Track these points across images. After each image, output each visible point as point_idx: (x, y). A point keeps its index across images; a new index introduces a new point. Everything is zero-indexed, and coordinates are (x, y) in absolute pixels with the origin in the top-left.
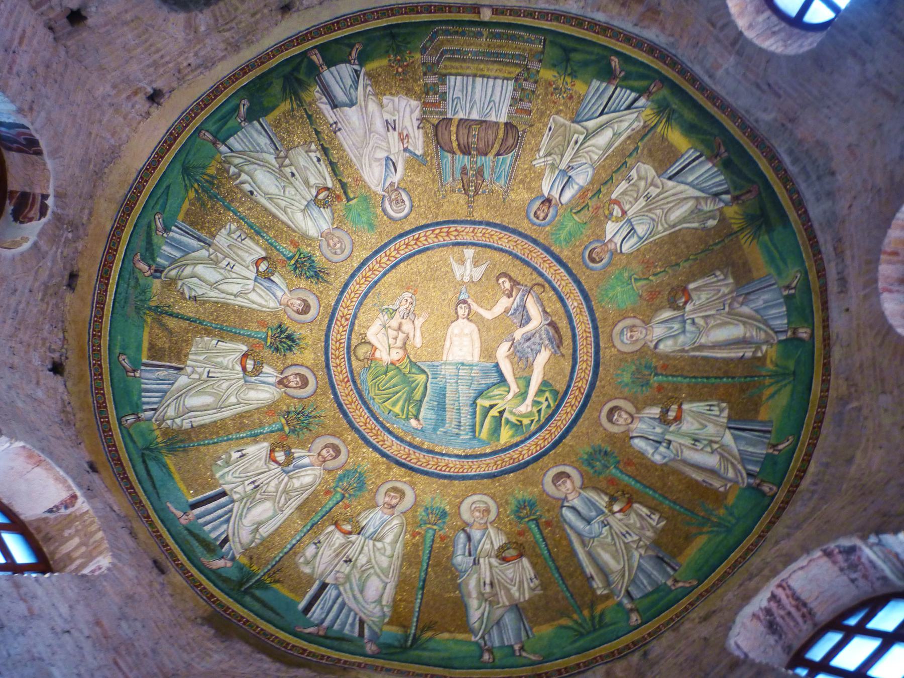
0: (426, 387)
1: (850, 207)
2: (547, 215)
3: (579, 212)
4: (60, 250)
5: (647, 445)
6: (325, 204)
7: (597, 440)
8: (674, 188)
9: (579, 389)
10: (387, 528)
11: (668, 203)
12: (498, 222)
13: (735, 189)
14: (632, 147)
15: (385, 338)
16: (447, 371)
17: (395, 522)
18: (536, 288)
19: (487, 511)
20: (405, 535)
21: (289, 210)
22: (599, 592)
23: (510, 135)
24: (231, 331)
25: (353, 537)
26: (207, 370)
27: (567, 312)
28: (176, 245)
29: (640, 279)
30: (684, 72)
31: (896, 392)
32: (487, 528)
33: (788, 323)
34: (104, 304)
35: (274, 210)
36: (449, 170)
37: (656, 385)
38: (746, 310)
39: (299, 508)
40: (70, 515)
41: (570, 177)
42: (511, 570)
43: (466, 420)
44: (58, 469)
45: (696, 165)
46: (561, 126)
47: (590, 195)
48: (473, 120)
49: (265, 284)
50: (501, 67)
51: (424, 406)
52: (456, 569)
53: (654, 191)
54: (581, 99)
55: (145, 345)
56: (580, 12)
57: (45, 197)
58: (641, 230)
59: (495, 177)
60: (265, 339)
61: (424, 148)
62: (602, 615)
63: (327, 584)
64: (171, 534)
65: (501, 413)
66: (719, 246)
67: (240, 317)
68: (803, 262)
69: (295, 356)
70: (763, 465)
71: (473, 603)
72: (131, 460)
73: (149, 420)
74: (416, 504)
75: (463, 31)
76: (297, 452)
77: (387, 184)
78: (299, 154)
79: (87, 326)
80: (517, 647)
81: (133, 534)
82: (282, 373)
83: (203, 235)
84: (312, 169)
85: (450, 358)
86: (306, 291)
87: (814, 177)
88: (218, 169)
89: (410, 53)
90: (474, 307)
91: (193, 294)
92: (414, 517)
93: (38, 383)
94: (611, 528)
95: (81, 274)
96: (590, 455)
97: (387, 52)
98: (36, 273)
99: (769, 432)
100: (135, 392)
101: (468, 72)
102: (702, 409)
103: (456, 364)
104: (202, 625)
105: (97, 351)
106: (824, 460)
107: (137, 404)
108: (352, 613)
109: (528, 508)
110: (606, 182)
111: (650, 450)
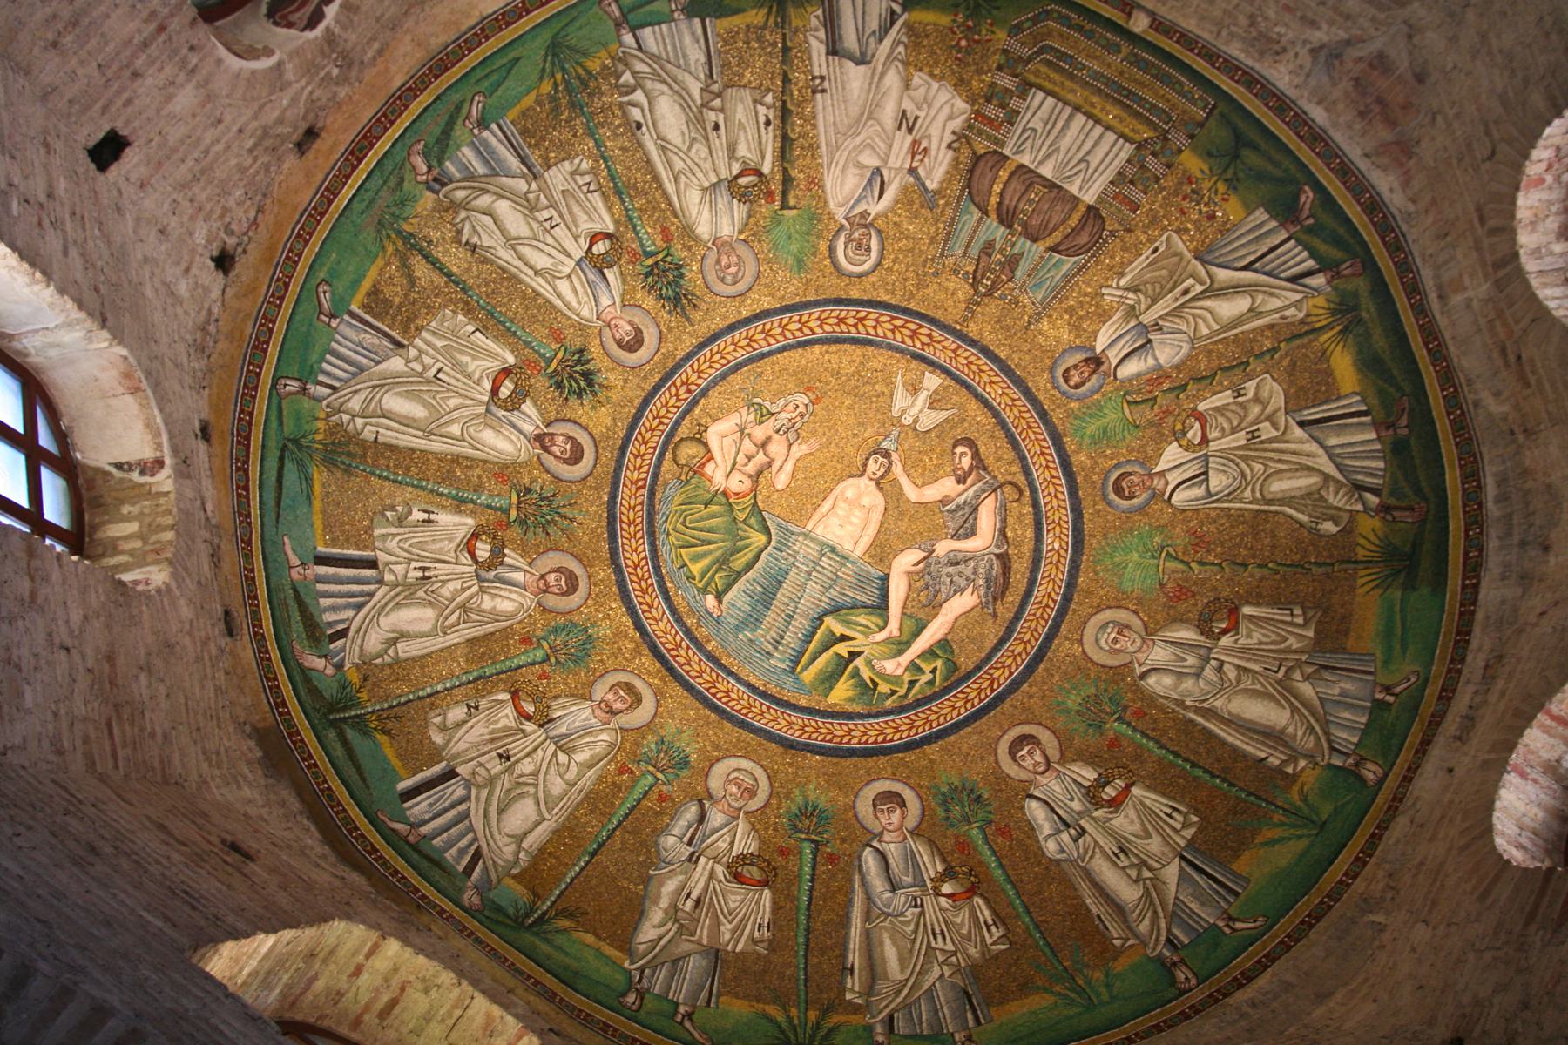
0: (758, 556)
1: (1543, 614)
2: (1083, 383)
4: (309, 88)
5: (1047, 819)
6: (742, 195)
7: (976, 773)
8: (1301, 442)
9: (993, 680)
10: (588, 739)
11: (1279, 461)
12: (1002, 355)
13: (1392, 494)
14: (1268, 344)
15: (734, 450)
16: (804, 549)
17: (604, 737)
18: (1008, 489)
19: (752, 792)
20: (609, 763)
21: (683, 179)
22: (848, 996)
23: (1088, 229)
24: (503, 324)
25: (530, 727)
26: (439, 365)
27: (1037, 551)
29: (1176, 559)
30: (1405, 267)
32: (738, 818)
34: (335, 196)
35: (660, 167)
36: (964, 235)
37: (1111, 734)
38: (1306, 689)
39: (472, 642)
40: (142, 485)
41: (1150, 341)
42: (739, 898)
43: (792, 639)
44: (156, 412)
45: (1352, 425)
46: (1176, 254)
49: (590, 276)
50: (1124, 115)
51: (741, 584)
53: (1267, 432)
54: (1224, 230)
55: (366, 285)
56: (1291, 93)
58: (1217, 482)
59: (1031, 282)
60: (549, 361)
61: (941, 183)
62: (831, 1031)
63: (458, 775)
65: (854, 655)
67: (527, 308)
69: (580, 409)
70: (1197, 938)
71: (656, 915)
72: (263, 446)
73: (319, 400)
74: (648, 726)
75: (1091, 31)
76: (511, 557)
77: (856, 211)
78: (742, 100)
79: (297, 217)
80: (682, 1009)
81: (215, 558)
82: (548, 426)
83: (534, 157)
84: (751, 132)
85: (819, 530)
86: (649, 317)
87: (1516, 539)
88: (604, 67)
89: (991, 25)
90: (898, 470)
91: (475, 240)
92: (637, 744)
93: (187, 270)
94: (922, 913)
95: (324, 135)
97: (957, 6)
98: (261, 108)
99: (1237, 894)
101: (1070, 97)
102: (1157, 808)
103: (823, 544)
104: (250, 737)
105: (292, 261)
106: (1289, 977)
107: (312, 366)
108: (470, 836)
110: (1204, 378)
111: (1047, 829)
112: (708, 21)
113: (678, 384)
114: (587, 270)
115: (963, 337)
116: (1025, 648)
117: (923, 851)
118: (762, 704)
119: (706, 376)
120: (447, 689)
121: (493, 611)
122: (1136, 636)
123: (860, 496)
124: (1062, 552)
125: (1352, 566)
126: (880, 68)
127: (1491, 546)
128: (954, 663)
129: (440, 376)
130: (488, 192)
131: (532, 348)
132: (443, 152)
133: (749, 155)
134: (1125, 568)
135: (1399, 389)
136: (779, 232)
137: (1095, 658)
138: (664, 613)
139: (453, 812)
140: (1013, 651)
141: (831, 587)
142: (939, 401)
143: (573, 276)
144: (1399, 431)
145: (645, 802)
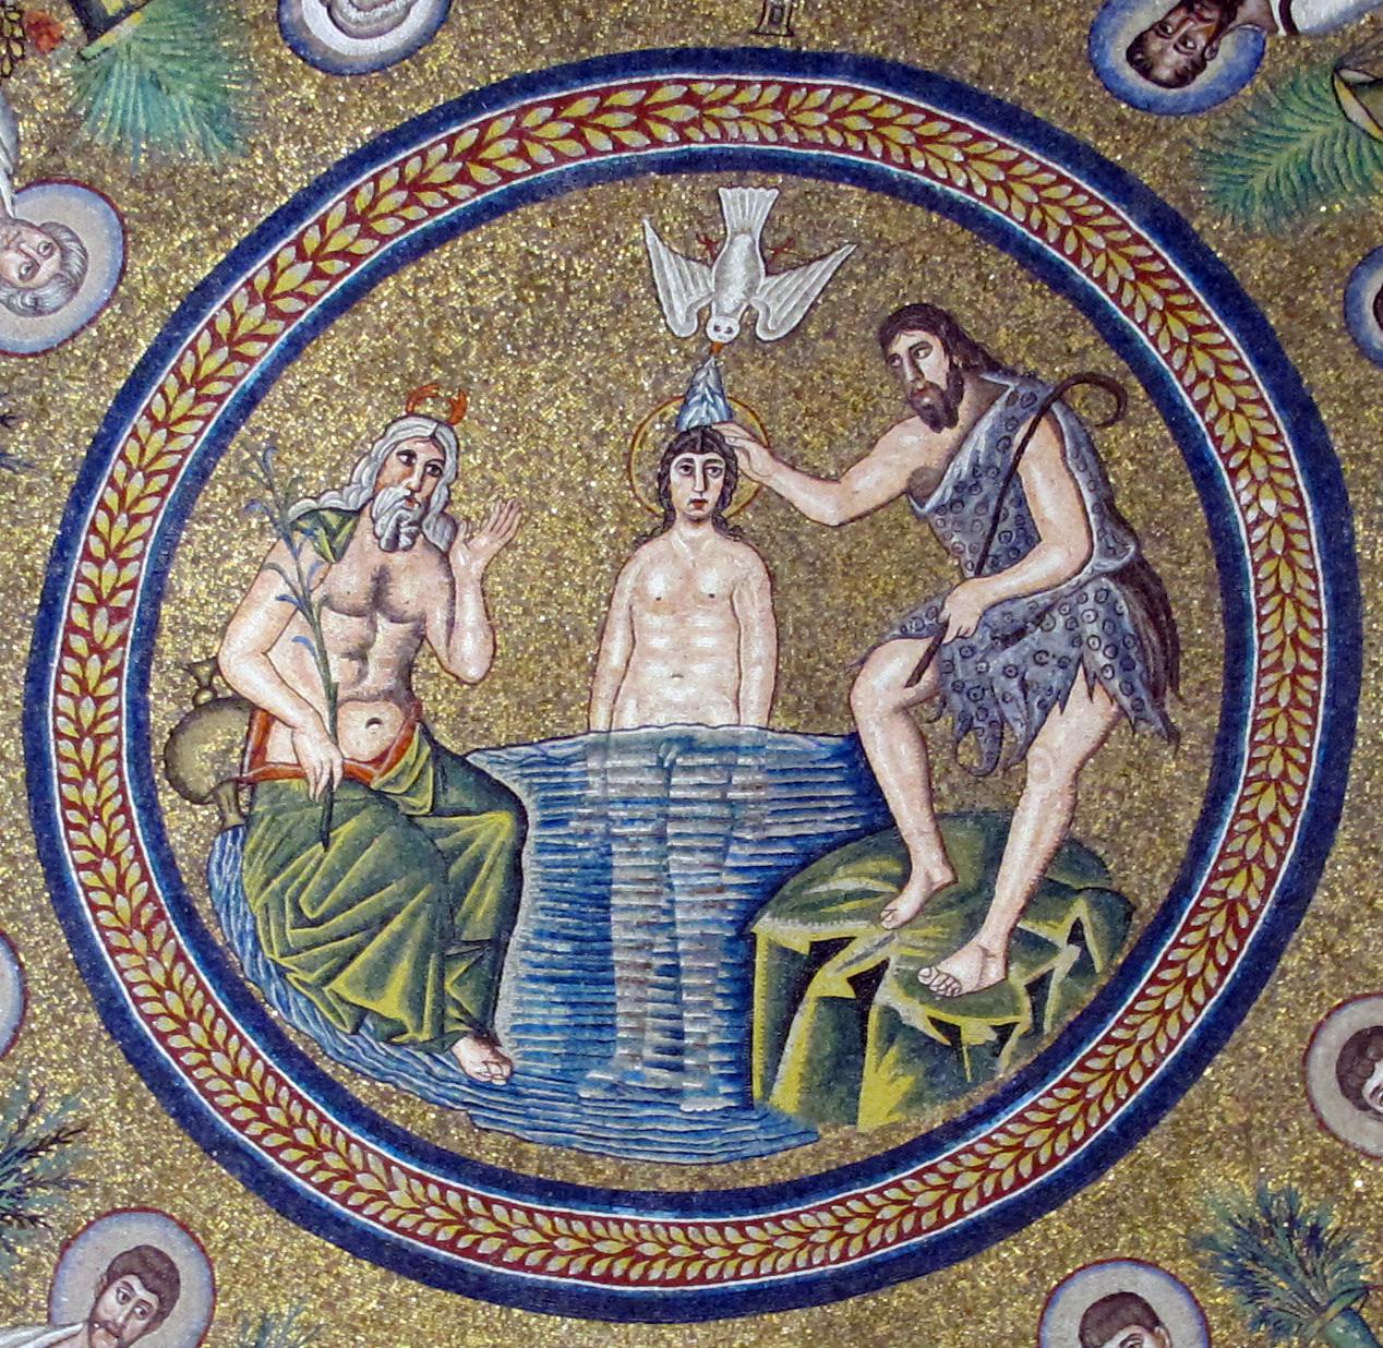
0: (516, 872)
9: (1233, 903)
15: (311, 662)
43: (704, 1027)
51: (515, 964)
65: (867, 983)
85: (629, 718)
90: (756, 462)
103: (653, 745)
113: (80, 618)
116: (1282, 799)
118: (720, 1228)
119: (135, 549)
123: (689, 577)
128: (1118, 894)
136: (120, 95)
138: (388, 1164)
140: (1254, 815)
141: (728, 840)
142: (791, 242)
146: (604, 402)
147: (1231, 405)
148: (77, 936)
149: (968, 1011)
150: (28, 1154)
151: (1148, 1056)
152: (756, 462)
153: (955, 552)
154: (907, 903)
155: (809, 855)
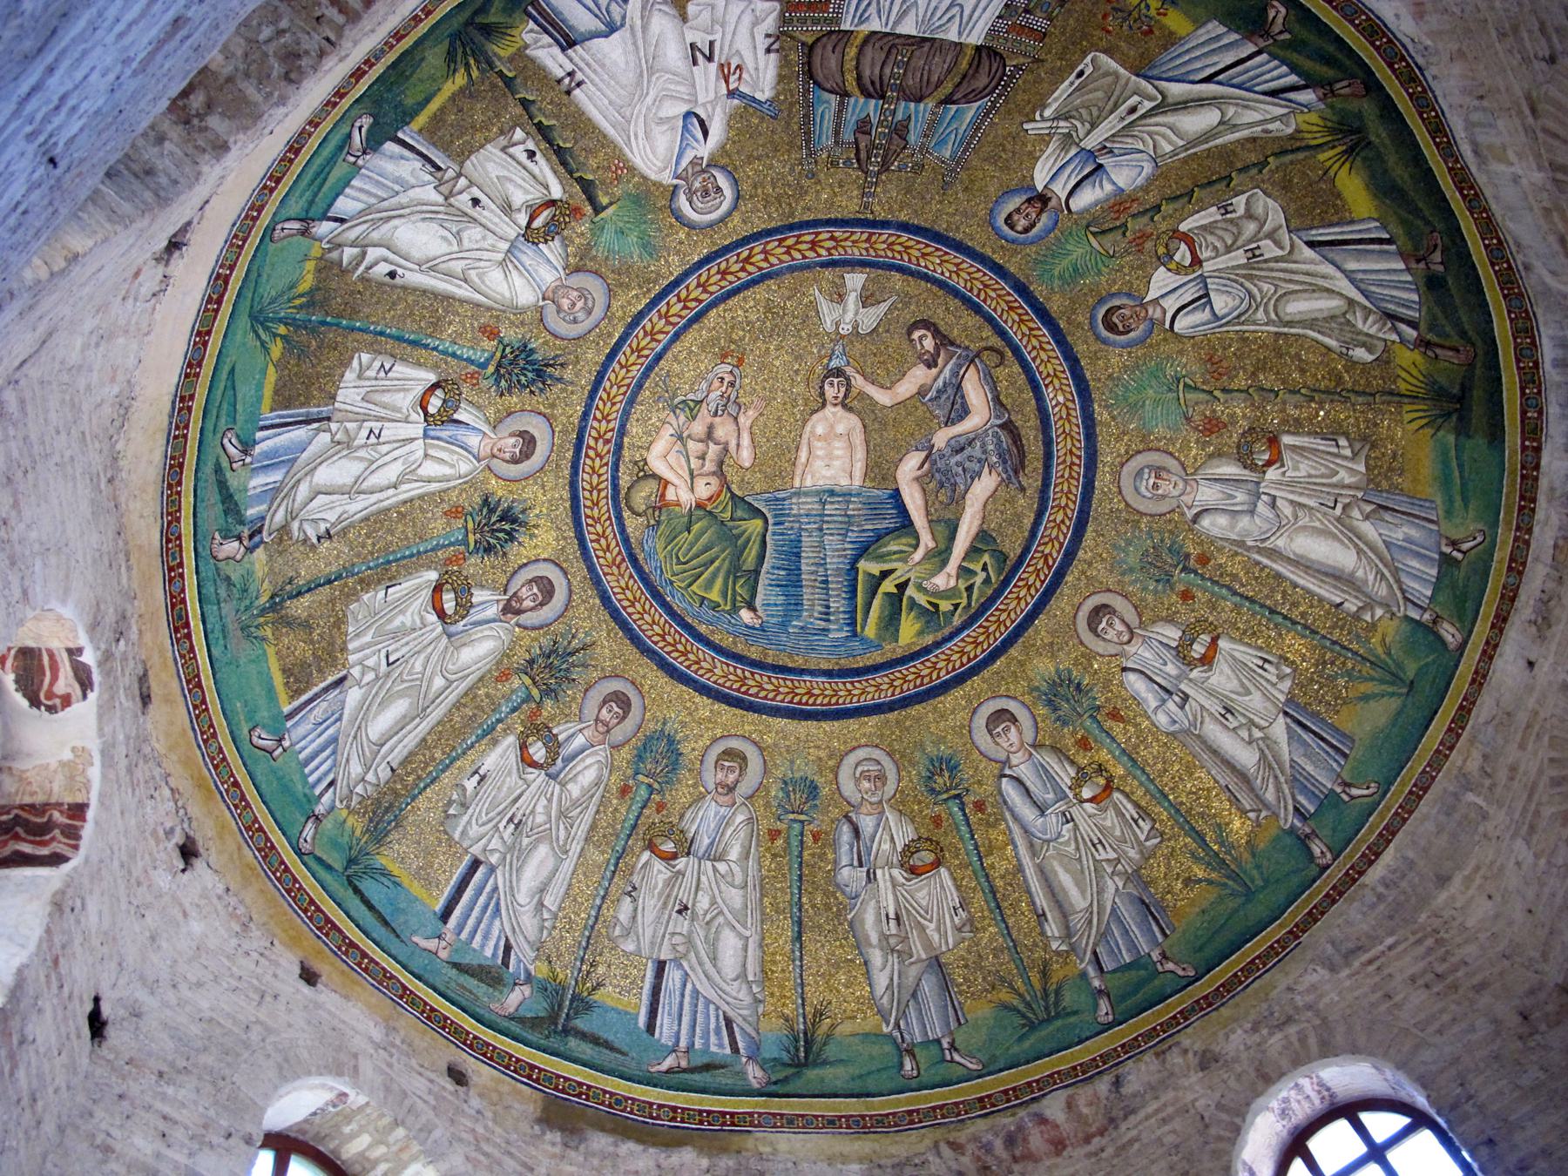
0: (764, 543)
2: (1033, 225)
3: (1103, 232)
5: (1149, 691)
6: (548, 234)
8: (1312, 262)
9: (1046, 557)
10: (729, 832)
11: (1291, 281)
13: (1431, 329)
14: (1253, 158)
15: (683, 460)
17: (740, 818)
19: (881, 778)
21: (473, 274)
22: (1054, 945)
25: (681, 863)
28: (273, 461)
29: (1196, 389)
31: (1543, 861)
32: (882, 813)
33: (1431, 599)
34: (198, 676)
38: (1367, 528)
41: (1100, 166)
42: (925, 892)
43: (838, 604)
45: (1373, 251)
46: (1107, 74)
47: (1135, 208)
48: (900, 36)
49: (444, 434)
51: (763, 580)
52: (843, 893)
54: (1171, 40)
55: (278, 680)
57: (74, 652)
58: (1221, 303)
60: (465, 542)
64: (441, 994)
65: (902, 587)
66: (1360, 399)
68: (1495, 524)
69: (521, 551)
71: (876, 957)
72: (339, 905)
73: (332, 808)
76: (562, 731)
77: (684, 163)
78: (488, 159)
79: (191, 734)
82: (505, 592)
84: (518, 176)
85: (808, 483)
88: (319, 270)
90: (858, 382)
91: (323, 527)
92: (767, 805)
93: (185, 914)
94: (1076, 827)
96: (1053, 685)
99: (1345, 756)
100: (296, 777)
103: (818, 493)
104: (544, 1133)
105: (220, 763)
106: (1411, 854)
108: (712, 1007)
109: (947, 774)
112: (400, 135)
113: (592, 443)
114: (439, 434)
115: (874, 224)
117: (1051, 761)
120: (603, 898)
121: (585, 792)
122: (1174, 478)
123: (832, 427)
124: (1070, 405)
125: (1397, 399)
126: (639, 22)
127: (1551, 411)
129: (392, 659)
130: (299, 481)
131: (444, 546)
132: (238, 512)
133: (529, 197)
134: (1143, 406)
135: (1428, 223)
136: (607, 237)
137: (1141, 508)
139: (687, 999)
143: (431, 452)
144: (1432, 267)
145: (806, 853)
146: (798, 358)
147: (1045, 357)
148: (591, 568)
149: (942, 598)
150: (572, 654)
151: (1013, 616)
152: (858, 382)
153: (937, 417)
154: (918, 555)
155: (879, 536)
